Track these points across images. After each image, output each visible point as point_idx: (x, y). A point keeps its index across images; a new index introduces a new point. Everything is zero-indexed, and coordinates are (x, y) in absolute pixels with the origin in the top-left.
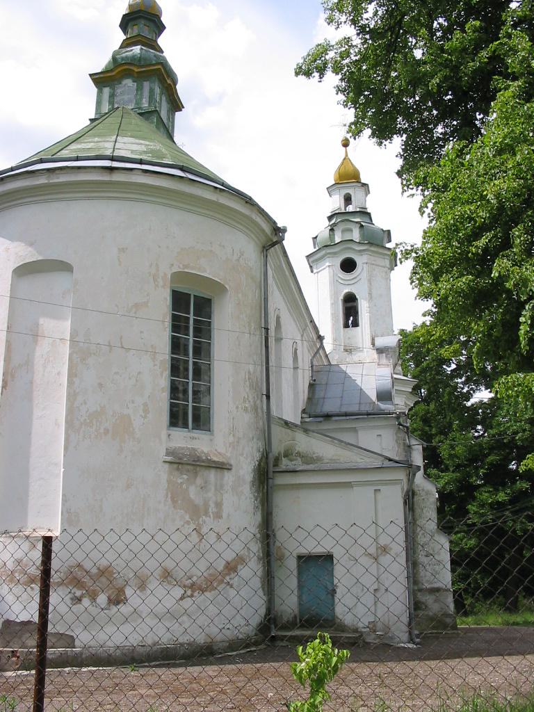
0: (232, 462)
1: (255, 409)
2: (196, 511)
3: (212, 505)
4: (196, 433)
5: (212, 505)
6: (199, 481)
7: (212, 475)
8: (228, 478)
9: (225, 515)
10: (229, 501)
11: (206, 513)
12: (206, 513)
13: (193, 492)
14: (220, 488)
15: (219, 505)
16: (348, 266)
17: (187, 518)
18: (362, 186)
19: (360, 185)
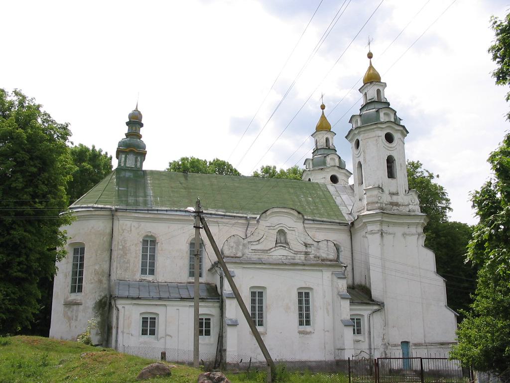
0: (83, 302)
1: (100, 281)
2: (70, 319)
3: (74, 317)
4: (79, 294)
5: (74, 317)
6: (71, 309)
7: (75, 307)
8: (81, 307)
9: (78, 320)
10: (81, 315)
11: (72, 320)
12: (72, 320)
13: (69, 313)
14: (77, 311)
15: (77, 317)
16: (358, 144)
17: (67, 321)
18: (371, 84)
19: (369, 84)
